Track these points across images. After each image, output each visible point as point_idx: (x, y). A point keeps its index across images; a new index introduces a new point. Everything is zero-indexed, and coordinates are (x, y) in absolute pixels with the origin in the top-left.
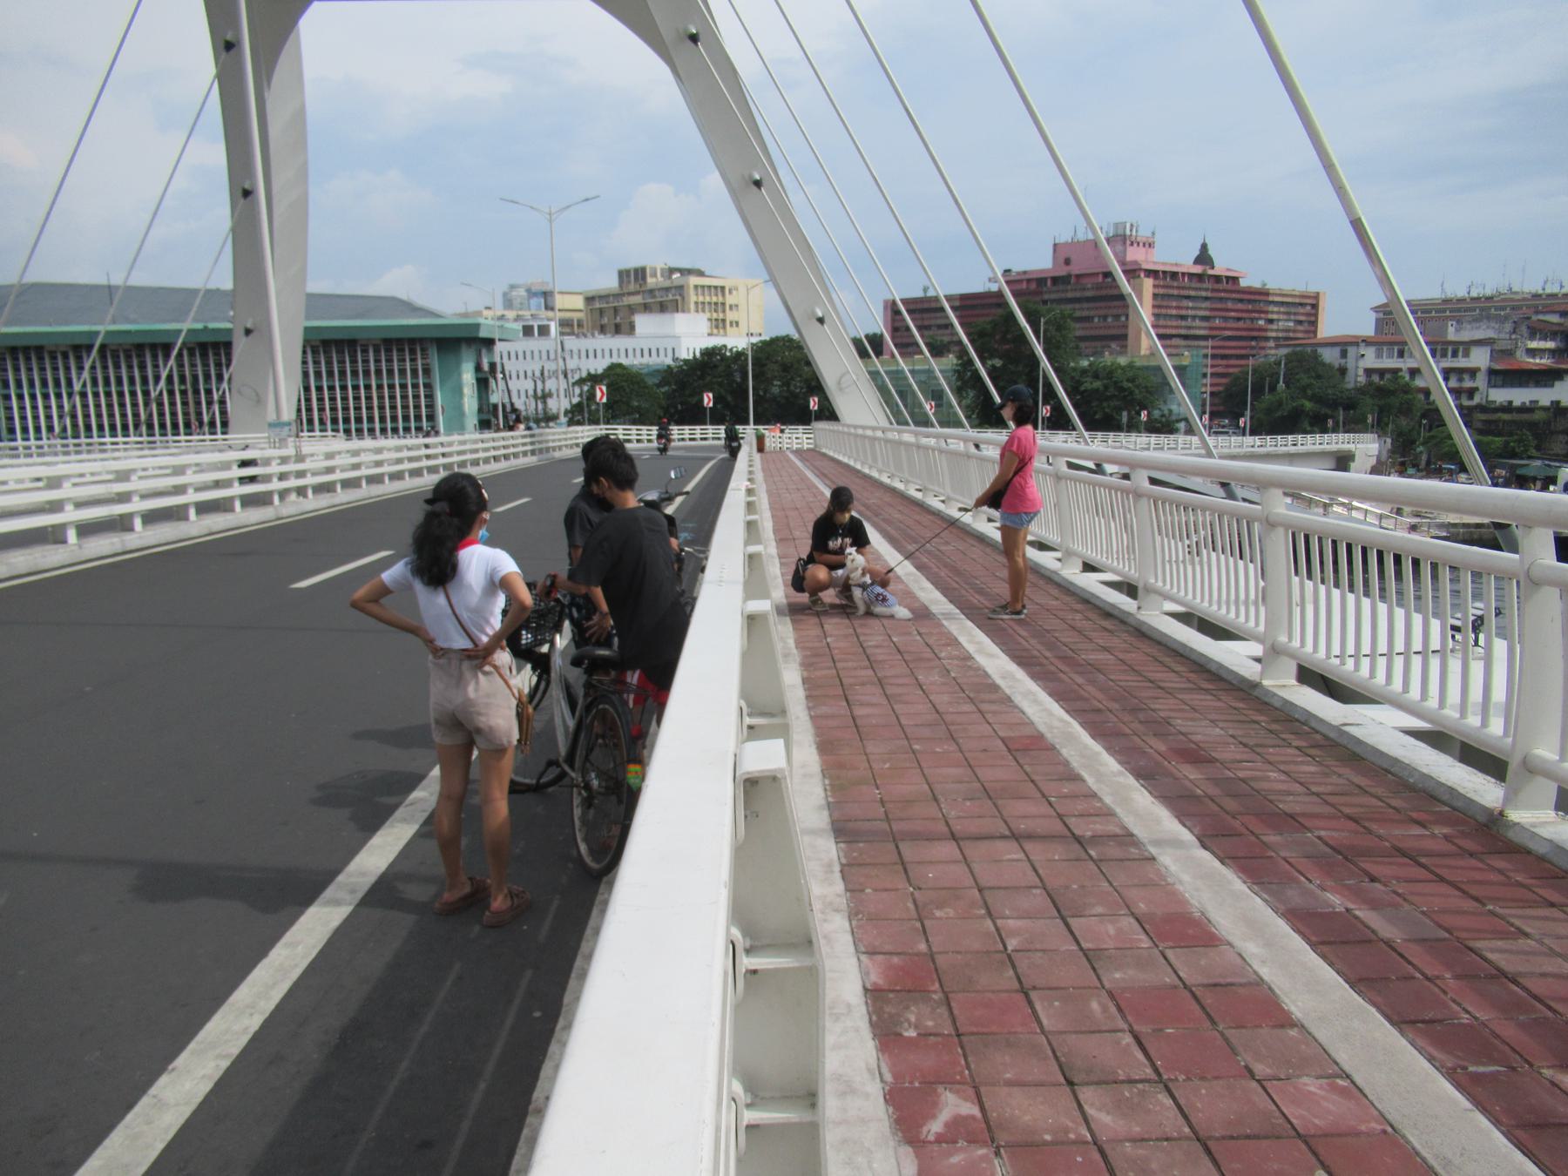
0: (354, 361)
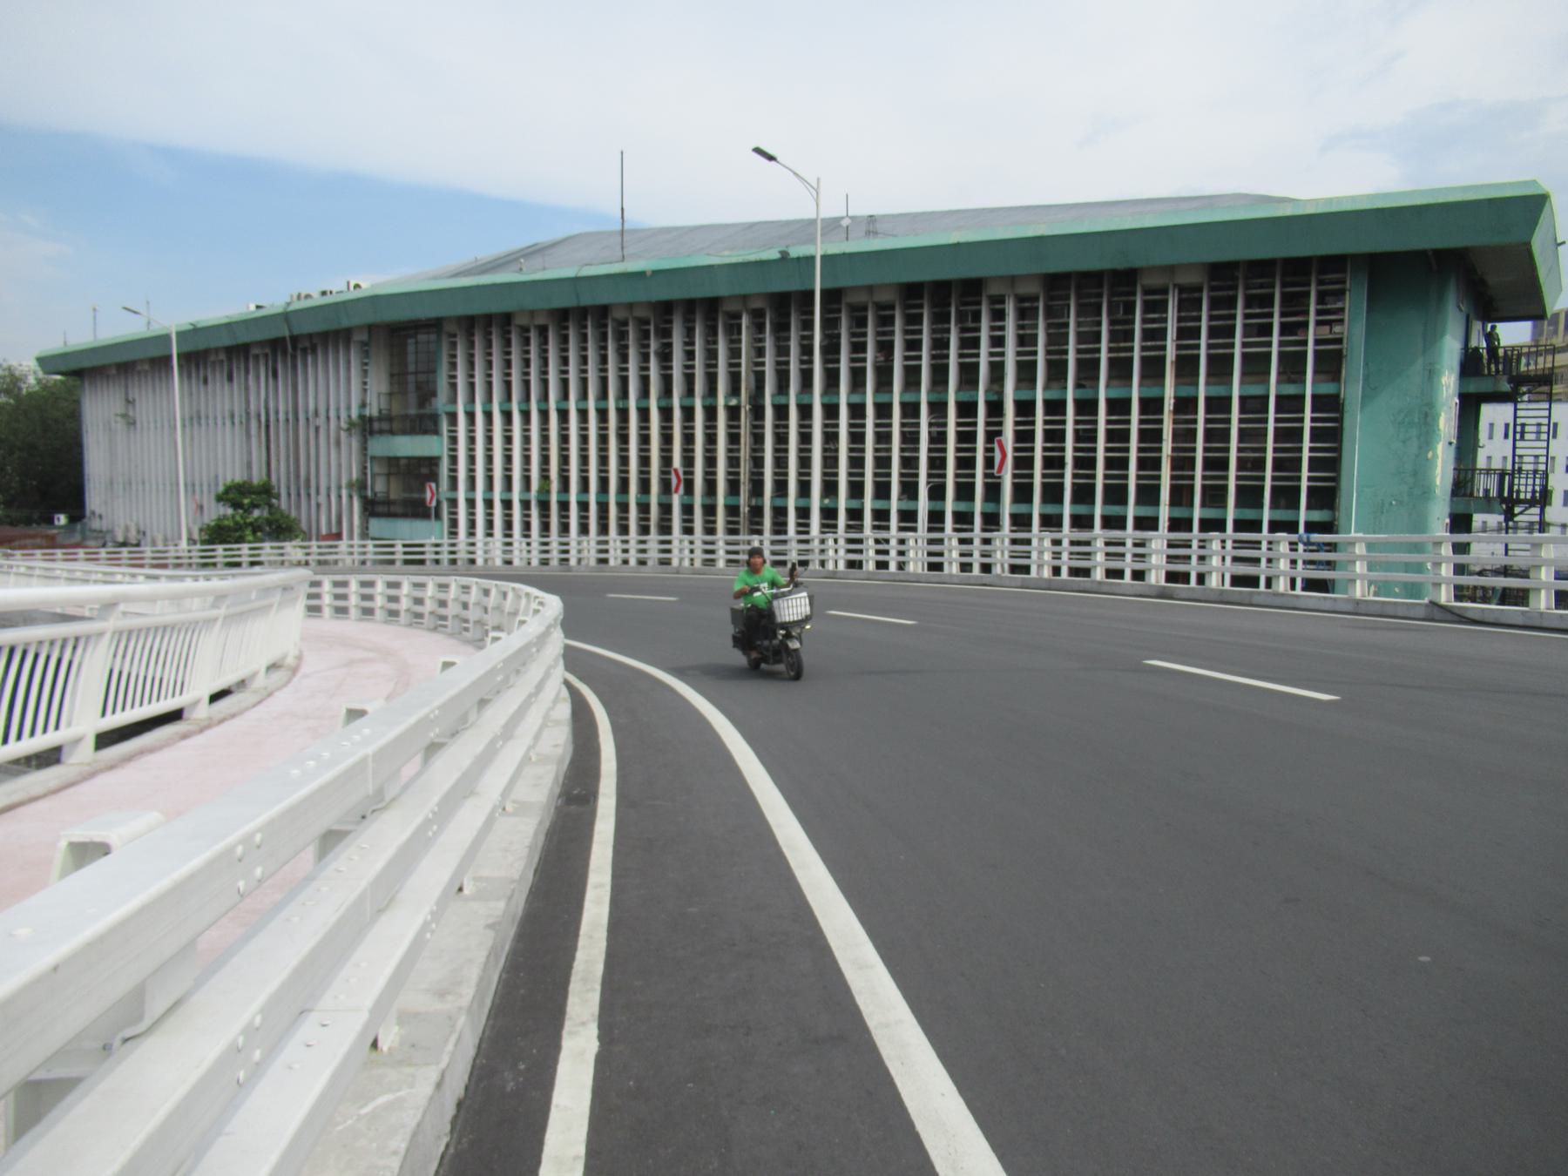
0: (1122, 335)
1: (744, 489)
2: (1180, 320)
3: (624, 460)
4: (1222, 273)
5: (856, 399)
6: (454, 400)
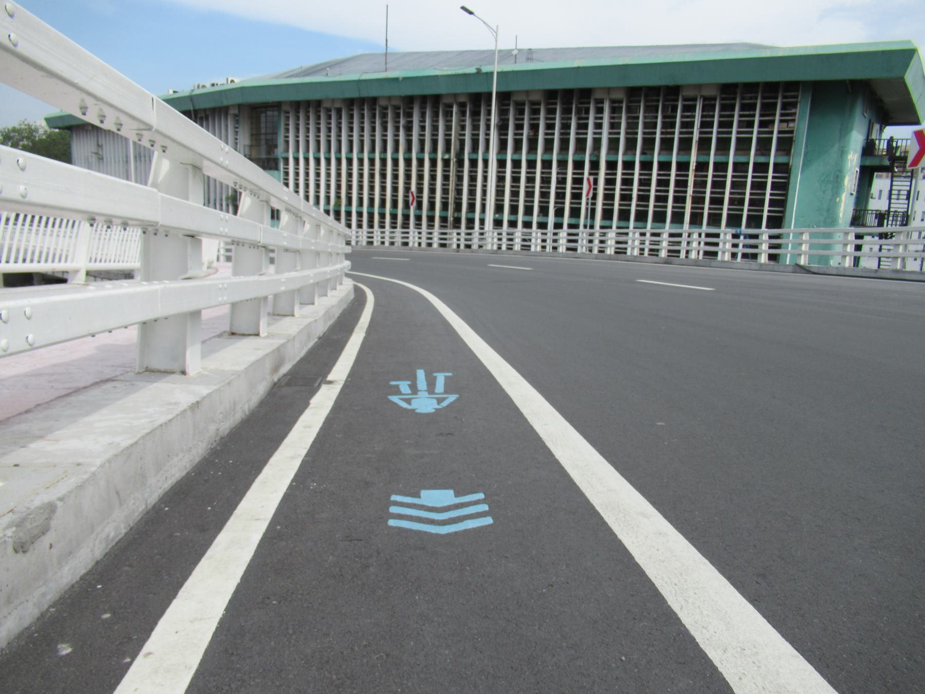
0: (669, 125)
1: (451, 207)
2: (703, 116)
3: (383, 189)
4: (728, 90)
5: (516, 157)
6: (287, 150)
